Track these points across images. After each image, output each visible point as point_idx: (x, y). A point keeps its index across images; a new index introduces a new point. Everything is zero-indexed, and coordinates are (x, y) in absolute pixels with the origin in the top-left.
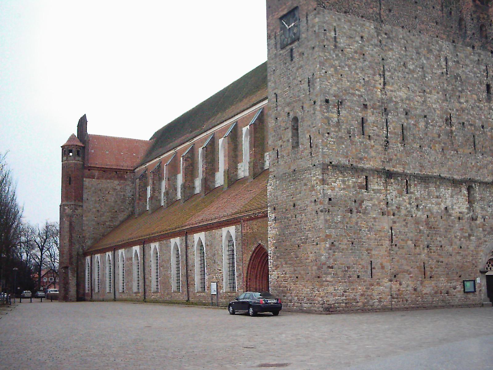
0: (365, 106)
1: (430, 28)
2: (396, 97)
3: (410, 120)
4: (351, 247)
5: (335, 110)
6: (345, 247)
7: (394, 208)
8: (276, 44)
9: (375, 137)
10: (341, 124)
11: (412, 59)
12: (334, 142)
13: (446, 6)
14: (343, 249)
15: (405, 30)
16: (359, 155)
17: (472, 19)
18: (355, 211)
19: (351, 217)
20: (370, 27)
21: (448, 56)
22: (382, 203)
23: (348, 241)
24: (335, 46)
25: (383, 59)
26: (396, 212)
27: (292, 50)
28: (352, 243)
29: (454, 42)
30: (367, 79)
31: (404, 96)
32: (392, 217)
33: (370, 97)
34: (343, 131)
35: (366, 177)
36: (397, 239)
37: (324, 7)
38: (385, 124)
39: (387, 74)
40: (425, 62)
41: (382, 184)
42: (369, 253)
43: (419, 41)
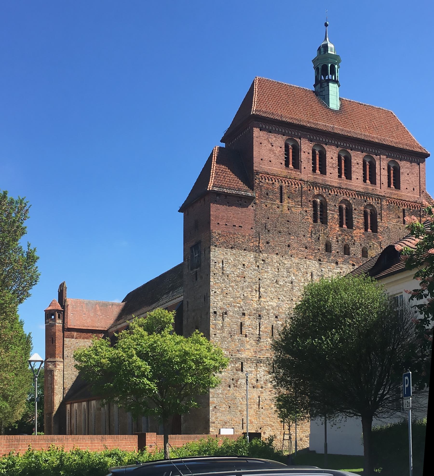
0: (244, 314)
1: (300, 252)
2: (268, 306)
3: (278, 322)
4: (228, 410)
5: (221, 318)
6: (224, 409)
7: (262, 383)
8: (188, 265)
9: (251, 335)
10: (225, 328)
11: (283, 277)
12: (219, 340)
13: (315, 234)
14: (222, 411)
15: (279, 256)
16: (238, 348)
17: (338, 241)
18: (232, 386)
19: (229, 390)
20: (251, 256)
21: (314, 272)
22: (253, 380)
23: (227, 406)
24: (223, 273)
25: (259, 279)
26: (264, 386)
27: (196, 272)
28: (230, 407)
29: (320, 260)
30: (245, 295)
31: (275, 304)
32: (261, 389)
33: (248, 307)
34: (226, 332)
35: (242, 363)
36: (263, 404)
37: (216, 246)
38: (258, 326)
39: (262, 289)
40: (294, 278)
41: (253, 367)
42: (241, 413)
43: (290, 262)
